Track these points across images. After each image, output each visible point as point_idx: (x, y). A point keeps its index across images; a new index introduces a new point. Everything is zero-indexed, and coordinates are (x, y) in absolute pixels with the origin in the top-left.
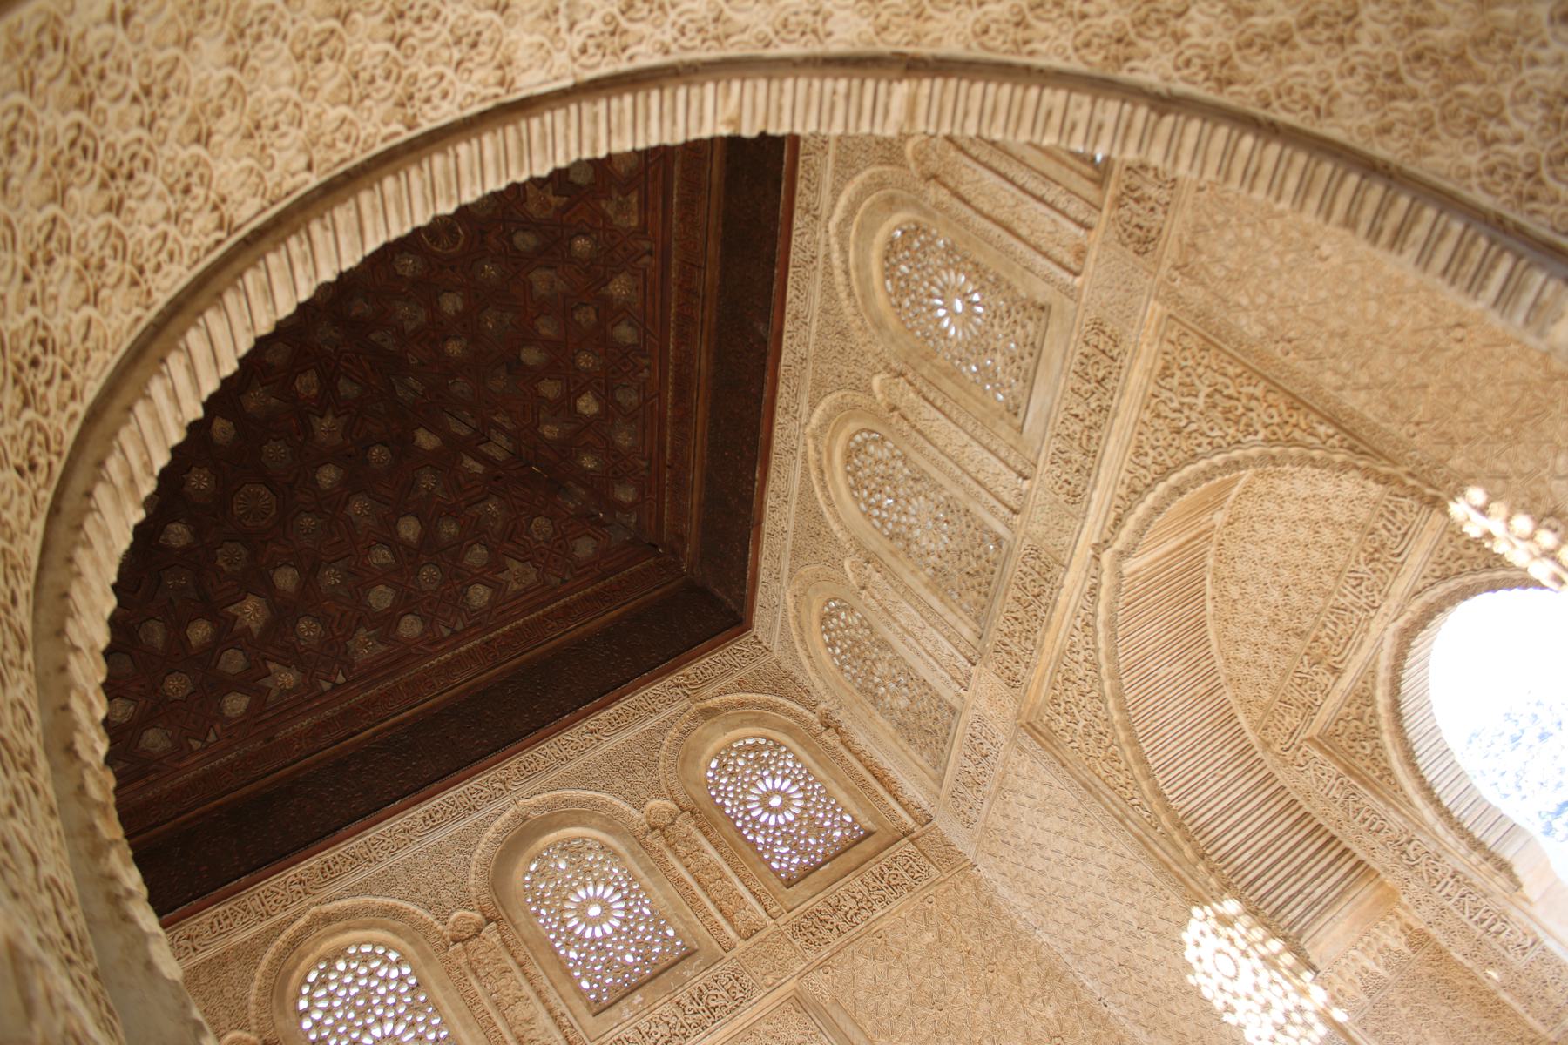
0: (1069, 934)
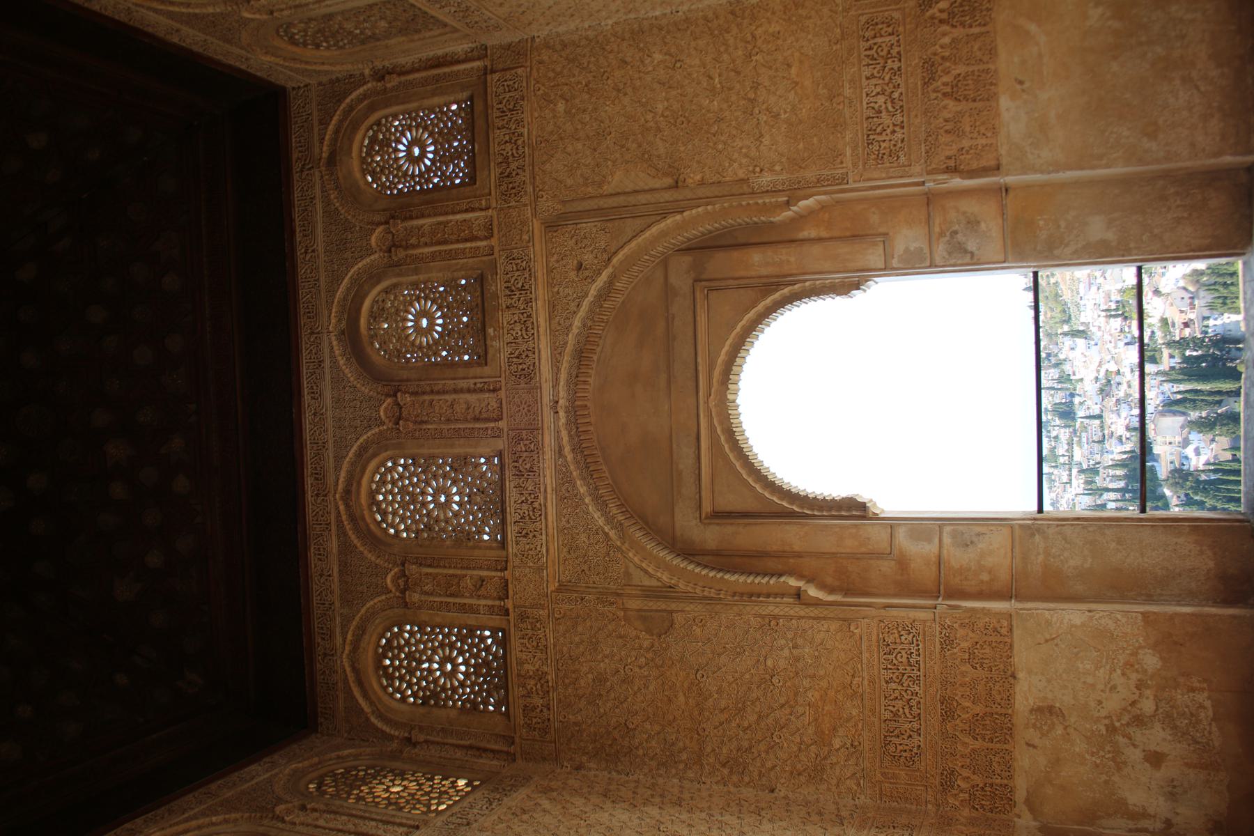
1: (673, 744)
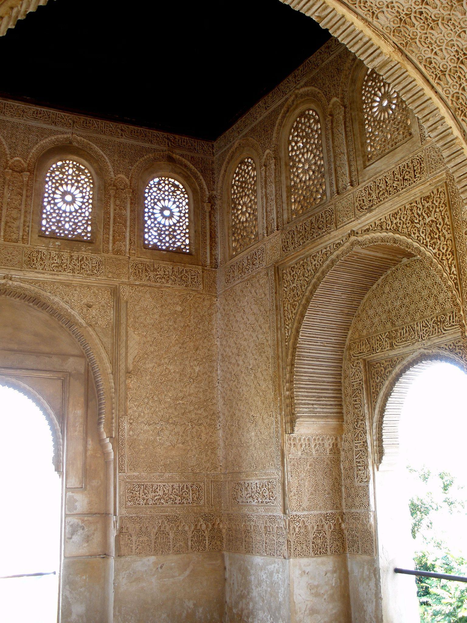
0: (227, 349)
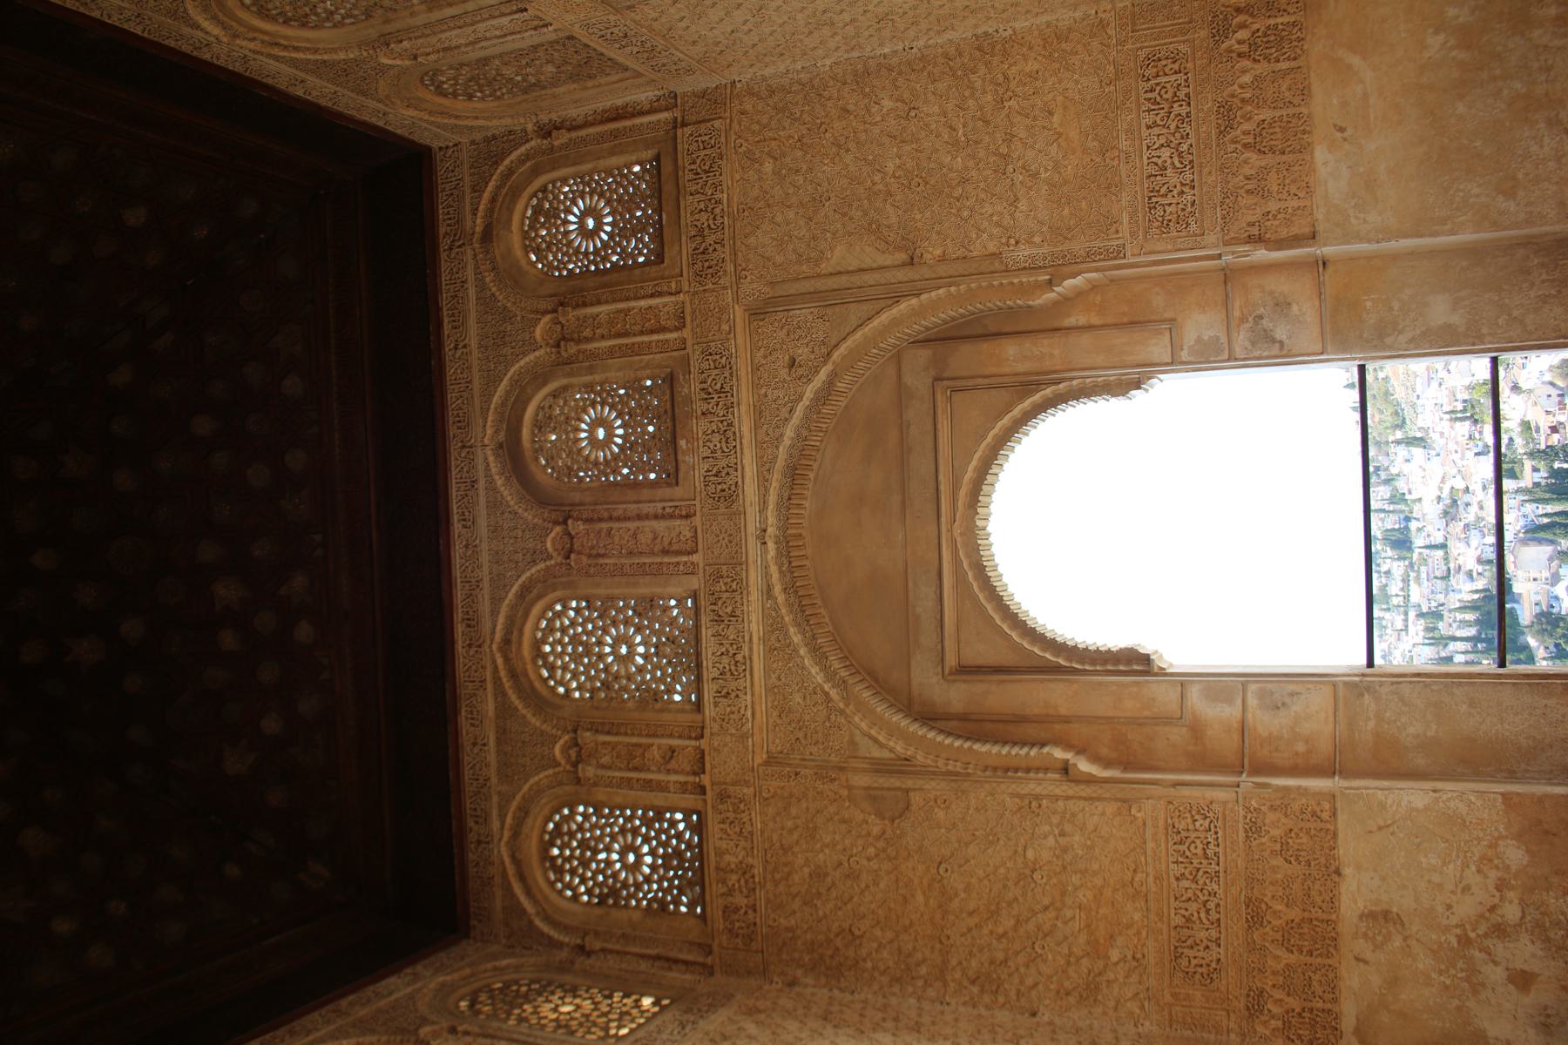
0: (832, 44)
1: (909, 955)
